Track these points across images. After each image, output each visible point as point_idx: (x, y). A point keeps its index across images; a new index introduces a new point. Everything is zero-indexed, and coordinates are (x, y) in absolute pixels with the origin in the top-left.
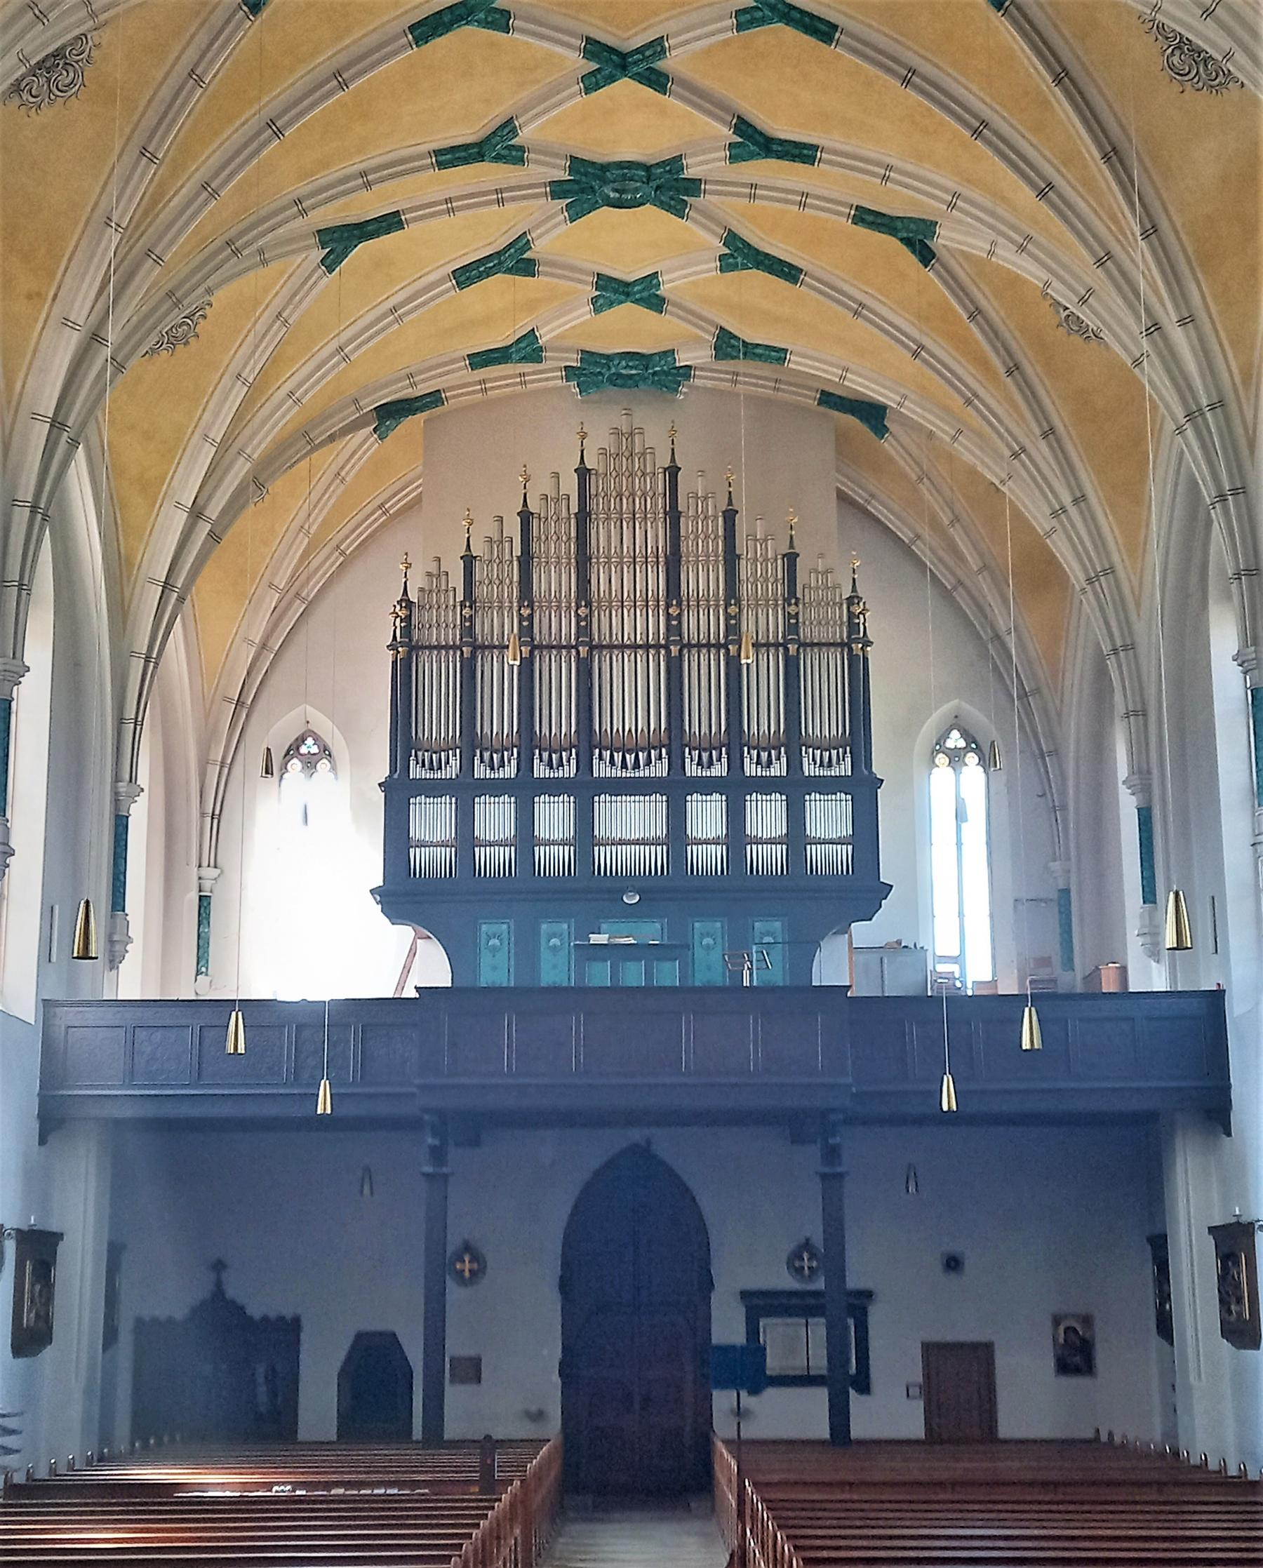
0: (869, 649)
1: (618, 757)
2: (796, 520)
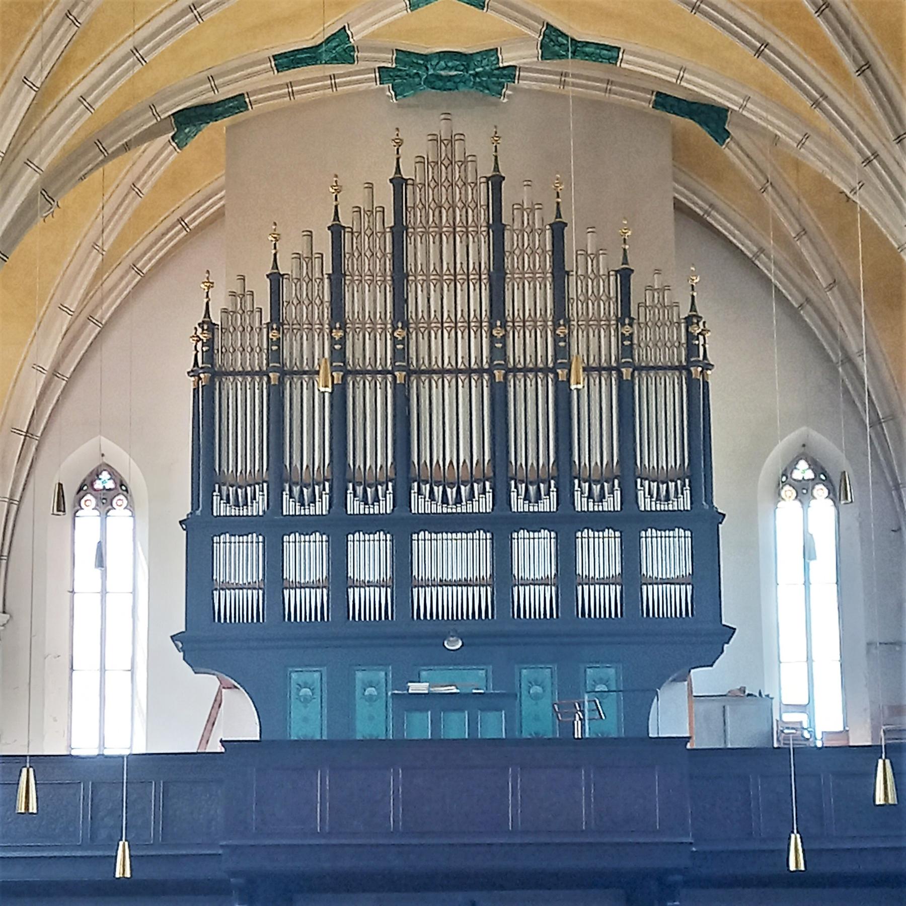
0: (709, 372)
1: (438, 491)
2: (629, 233)
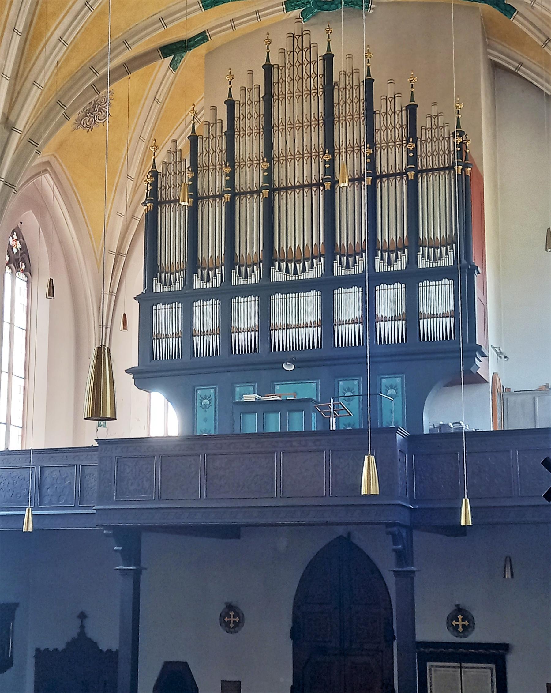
1: (291, 266)
